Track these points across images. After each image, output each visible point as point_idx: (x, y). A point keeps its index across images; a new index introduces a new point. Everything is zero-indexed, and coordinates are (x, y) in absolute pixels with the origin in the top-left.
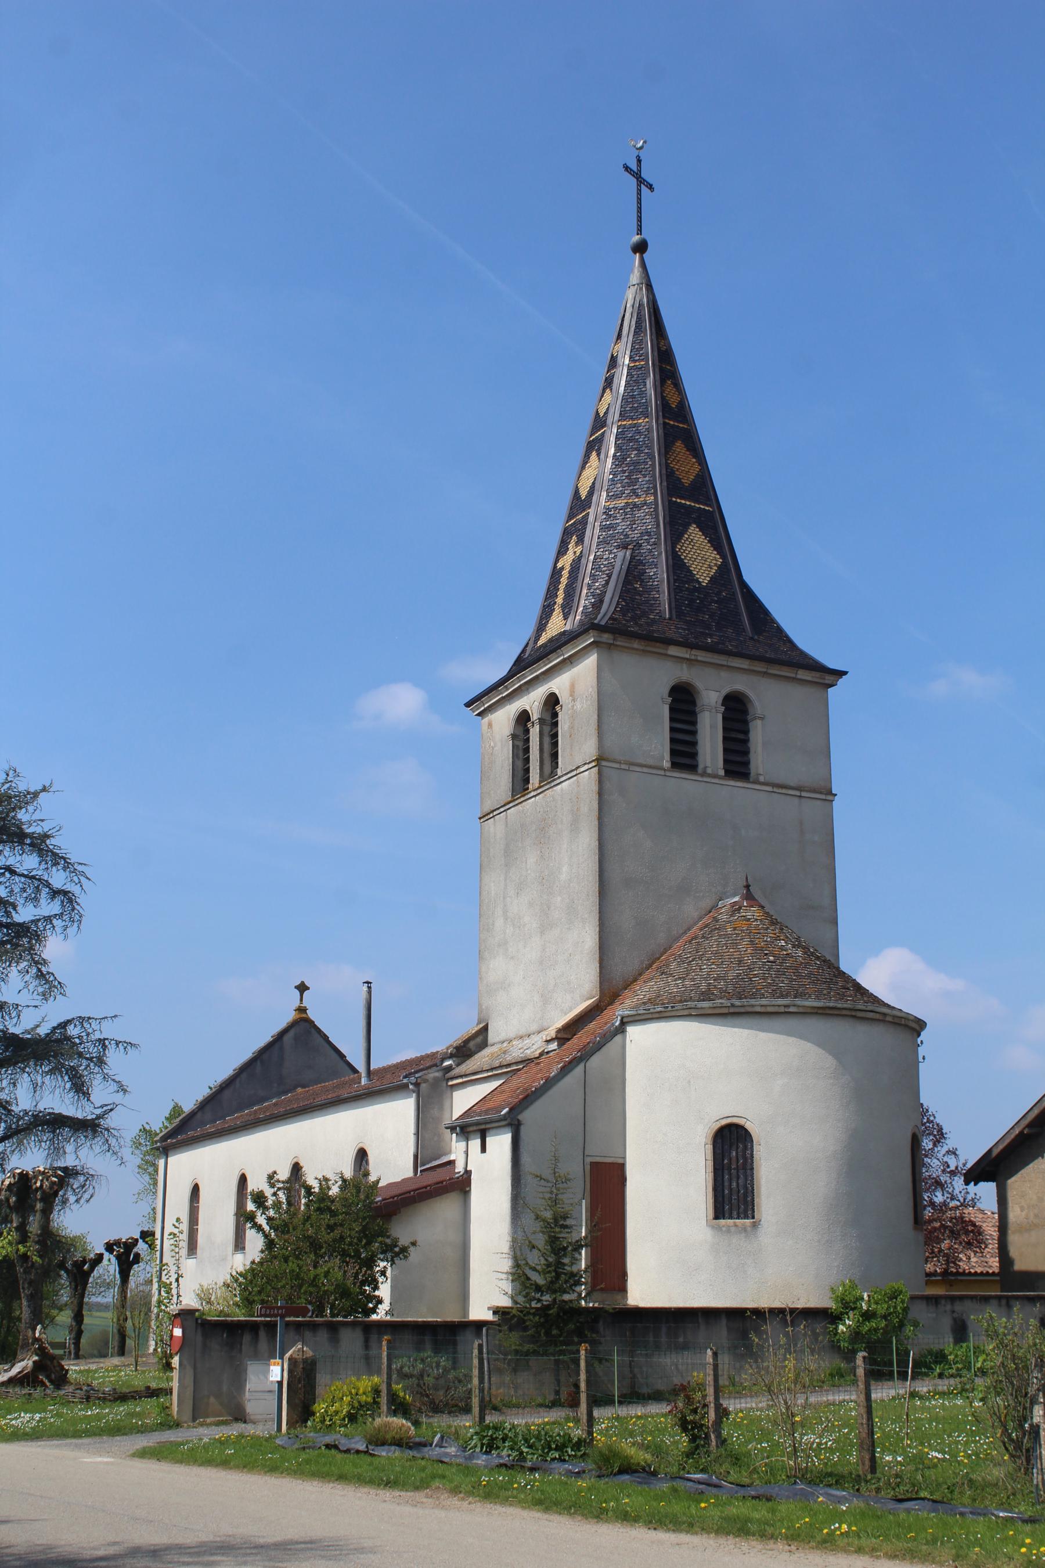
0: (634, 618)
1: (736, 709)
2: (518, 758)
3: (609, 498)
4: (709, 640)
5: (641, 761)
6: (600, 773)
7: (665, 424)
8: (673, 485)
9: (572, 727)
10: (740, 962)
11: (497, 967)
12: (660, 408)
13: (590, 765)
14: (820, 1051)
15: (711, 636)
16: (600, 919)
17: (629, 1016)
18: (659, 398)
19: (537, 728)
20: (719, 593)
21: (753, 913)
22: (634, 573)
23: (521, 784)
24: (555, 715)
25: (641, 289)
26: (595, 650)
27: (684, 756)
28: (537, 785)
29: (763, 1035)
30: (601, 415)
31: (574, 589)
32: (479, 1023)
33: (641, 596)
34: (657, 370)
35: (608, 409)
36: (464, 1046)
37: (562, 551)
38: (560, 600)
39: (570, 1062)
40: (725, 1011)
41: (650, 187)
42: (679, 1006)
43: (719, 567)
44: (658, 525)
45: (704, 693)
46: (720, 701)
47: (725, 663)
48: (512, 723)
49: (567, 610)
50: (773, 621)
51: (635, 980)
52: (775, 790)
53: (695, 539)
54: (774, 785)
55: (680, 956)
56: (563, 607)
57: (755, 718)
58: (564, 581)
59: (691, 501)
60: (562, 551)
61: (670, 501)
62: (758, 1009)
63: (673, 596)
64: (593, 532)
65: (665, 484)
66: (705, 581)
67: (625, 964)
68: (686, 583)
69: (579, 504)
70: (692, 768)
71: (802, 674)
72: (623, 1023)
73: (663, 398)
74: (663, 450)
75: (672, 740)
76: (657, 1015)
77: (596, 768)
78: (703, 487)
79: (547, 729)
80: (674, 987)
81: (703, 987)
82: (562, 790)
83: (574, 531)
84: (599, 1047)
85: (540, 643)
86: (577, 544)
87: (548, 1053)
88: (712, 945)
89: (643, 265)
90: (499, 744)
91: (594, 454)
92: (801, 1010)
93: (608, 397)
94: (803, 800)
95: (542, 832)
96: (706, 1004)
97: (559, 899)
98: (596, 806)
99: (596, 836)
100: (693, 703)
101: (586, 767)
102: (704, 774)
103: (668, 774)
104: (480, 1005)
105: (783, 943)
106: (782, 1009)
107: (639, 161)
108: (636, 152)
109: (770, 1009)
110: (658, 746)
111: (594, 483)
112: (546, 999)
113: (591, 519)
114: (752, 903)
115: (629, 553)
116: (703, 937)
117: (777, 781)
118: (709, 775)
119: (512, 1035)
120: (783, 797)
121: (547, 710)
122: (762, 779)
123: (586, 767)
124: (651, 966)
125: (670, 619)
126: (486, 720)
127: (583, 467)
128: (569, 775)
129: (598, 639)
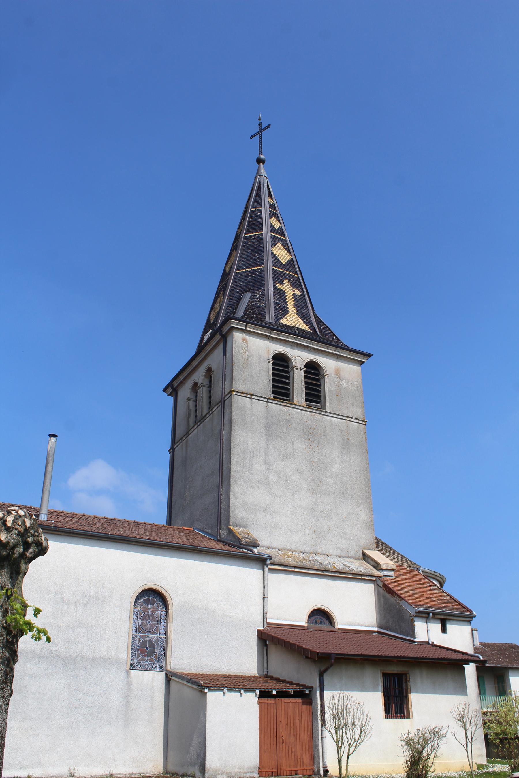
123: (357, 421)
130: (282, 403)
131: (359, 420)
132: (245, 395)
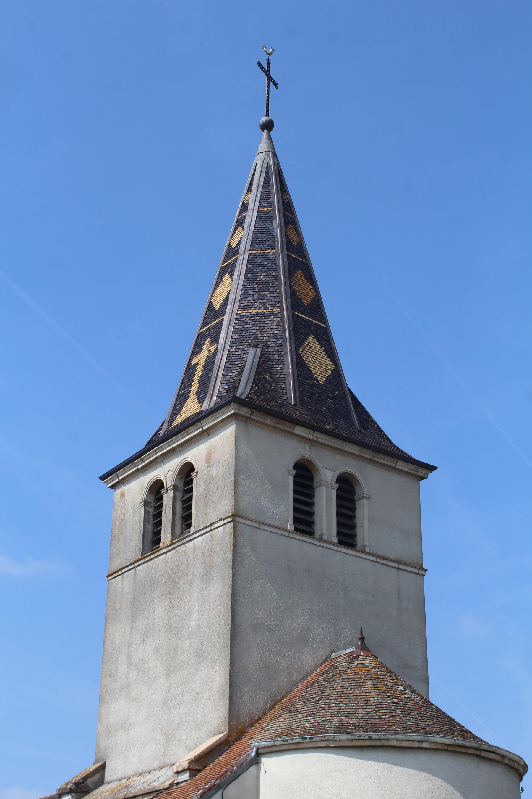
0: (265, 400)
1: (347, 487)
2: (148, 522)
3: (241, 308)
4: (327, 427)
5: (269, 522)
6: (235, 527)
7: (288, 255)
8: (296, 303)
9: (207, 490)
10: (367, 702)
11: (117, 710)
12: (285, 243)
13: (226, 521)
14: (450, 787)
15: (328, 423)
16: (231, 659)
17: (265, 747)
18: (284, 235)
19: (171, 494)
20: (333, 391)
21: (369, 661)
22: (264, 366)
23: (152, 541)
24: (191, 481)
25: (268, 155)
26: (234, 422)
27: (304, 521)
28: (169, 543)
29: (398, 770)
30: (234, 246)
31: (209, 379)
32: (96, 761)
33: (270, 385)
34: (282, 215)
35: (240, 242)
36: (83, 783)
37: (197, 349)
38: (195, 388)
39: (210, 789)
40: (363, 743)
41: (276, 85)
42: (317, 738)
43: (333, 371)
44: (284, 331)
45: (322, 471)
46: (335, 479)
47: (340, 447)
48: (145, 492)
49: (201, 396)
50: (374, 422)
51: (260, 719)
52: (378, 560)
53: (313, 348)
54: (377, 556)
55: (304, 697)
56: (198, 394)
57: (362, 498)
58: (199, 373)
59: (309, 320)
60: (197, 349)
61: (293, 314)
62: (394, 743)
63: (297, 387)
64: (225, 335)
65: (289, 300)
66: (322, 381)
67: (253, 701)
68: (307, 379)
69: (213, 314)
70: (311, 534)
71: (401, 465)
72: (258, 754)
73: (287, 237)
74: (287, 274)
75: (296, 510)
76: (294, 747)
77: (232, 523)
78: (316, 308)
79: (179, 495)
80: (306, 722)
81: (336, 722)
82: (195, 545)
83: (209, 331)
84: (236, 776)
85: (174, 424)
86: (211, 344)
87: (177, 784)
88: (336, 686)
89: (270, 138)
90: (131, 511)
91: (227, 275)
92: (433, 746)
93: (240, 233)
94: (401, 572)
95: (173, 584)
96: (344, 736)
97: (188, 643)
98: (230, 556)
99: (229, 583)
100: (312, 479)
101: (221, 523)
102: (321, 539)
103: (292, 535)
104: (98, 745)
105: (401, 688)
106: (416, 745)
107: (269, 64)
108: (267, 57)
109: (405, 744)
110: (284, 510)
111: (227, 298)
112: (169, 737)
113: (225, 324)
114: (368, 653)
115: (259, 351)
116: (325, 681)
117: (380, 553)
118: (325, 541)
119: (130, 772)
120: (384, 567)
121: (180, 479)
122: (367, 550)
123: (221, 523)
124: (273, 707)
125: (295, 405)
126: (118, 491)
127: (216, 286)
128: (203, 532)
129: (237, 412)
130: (147, 559)
131: (224, 519)
132: (117, 574)
